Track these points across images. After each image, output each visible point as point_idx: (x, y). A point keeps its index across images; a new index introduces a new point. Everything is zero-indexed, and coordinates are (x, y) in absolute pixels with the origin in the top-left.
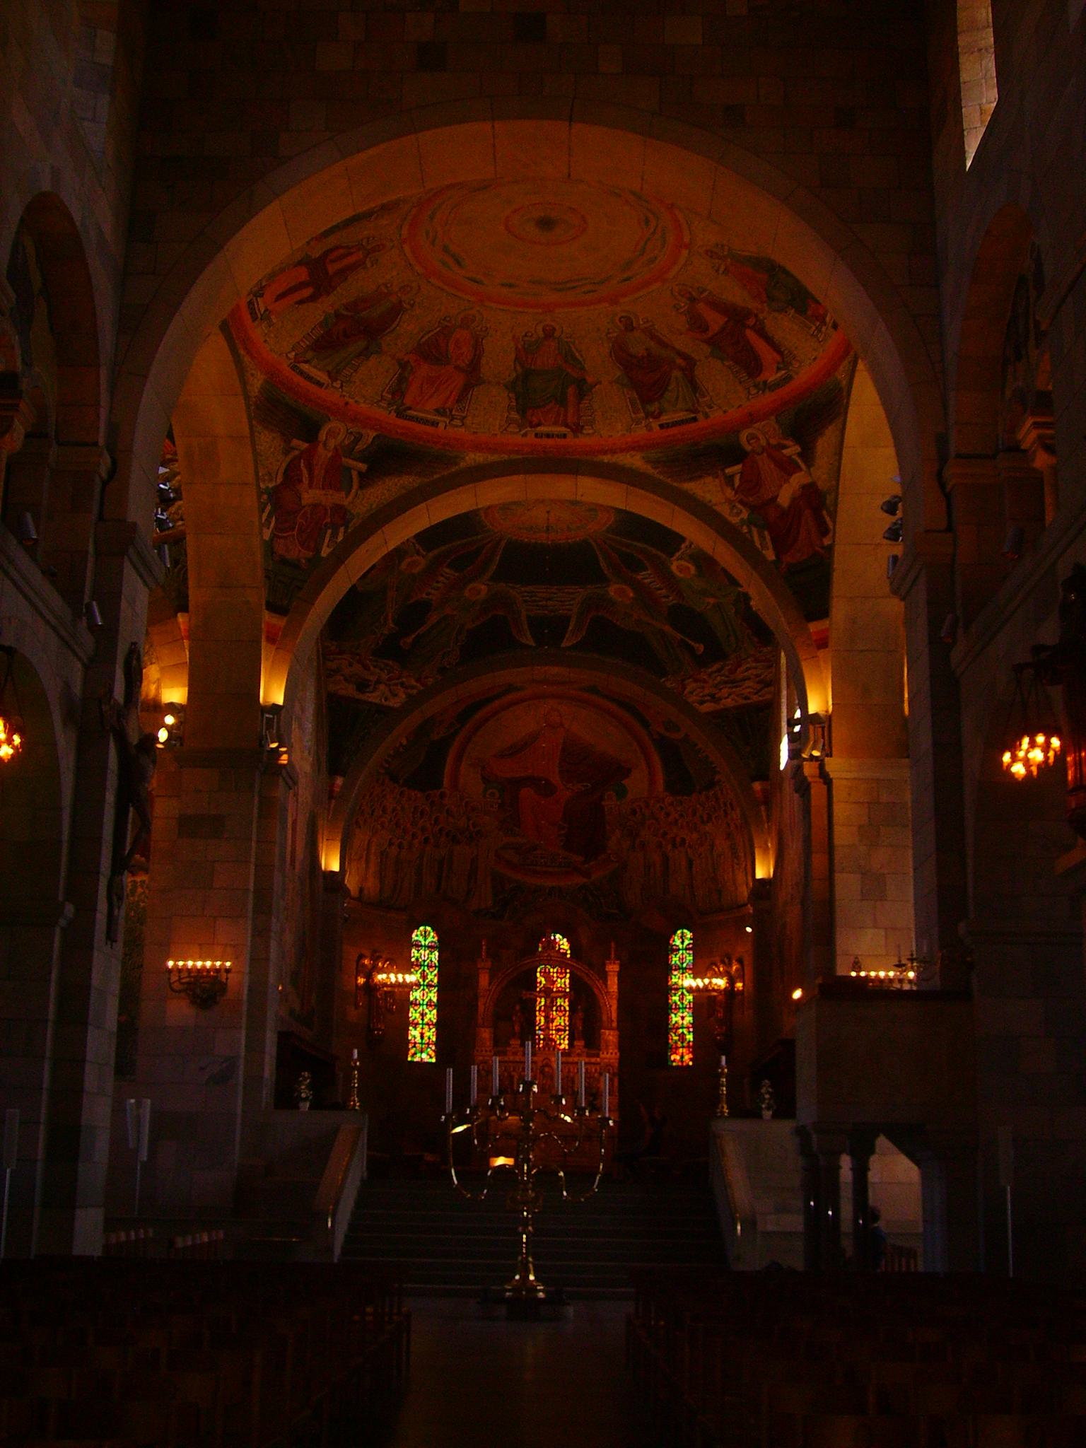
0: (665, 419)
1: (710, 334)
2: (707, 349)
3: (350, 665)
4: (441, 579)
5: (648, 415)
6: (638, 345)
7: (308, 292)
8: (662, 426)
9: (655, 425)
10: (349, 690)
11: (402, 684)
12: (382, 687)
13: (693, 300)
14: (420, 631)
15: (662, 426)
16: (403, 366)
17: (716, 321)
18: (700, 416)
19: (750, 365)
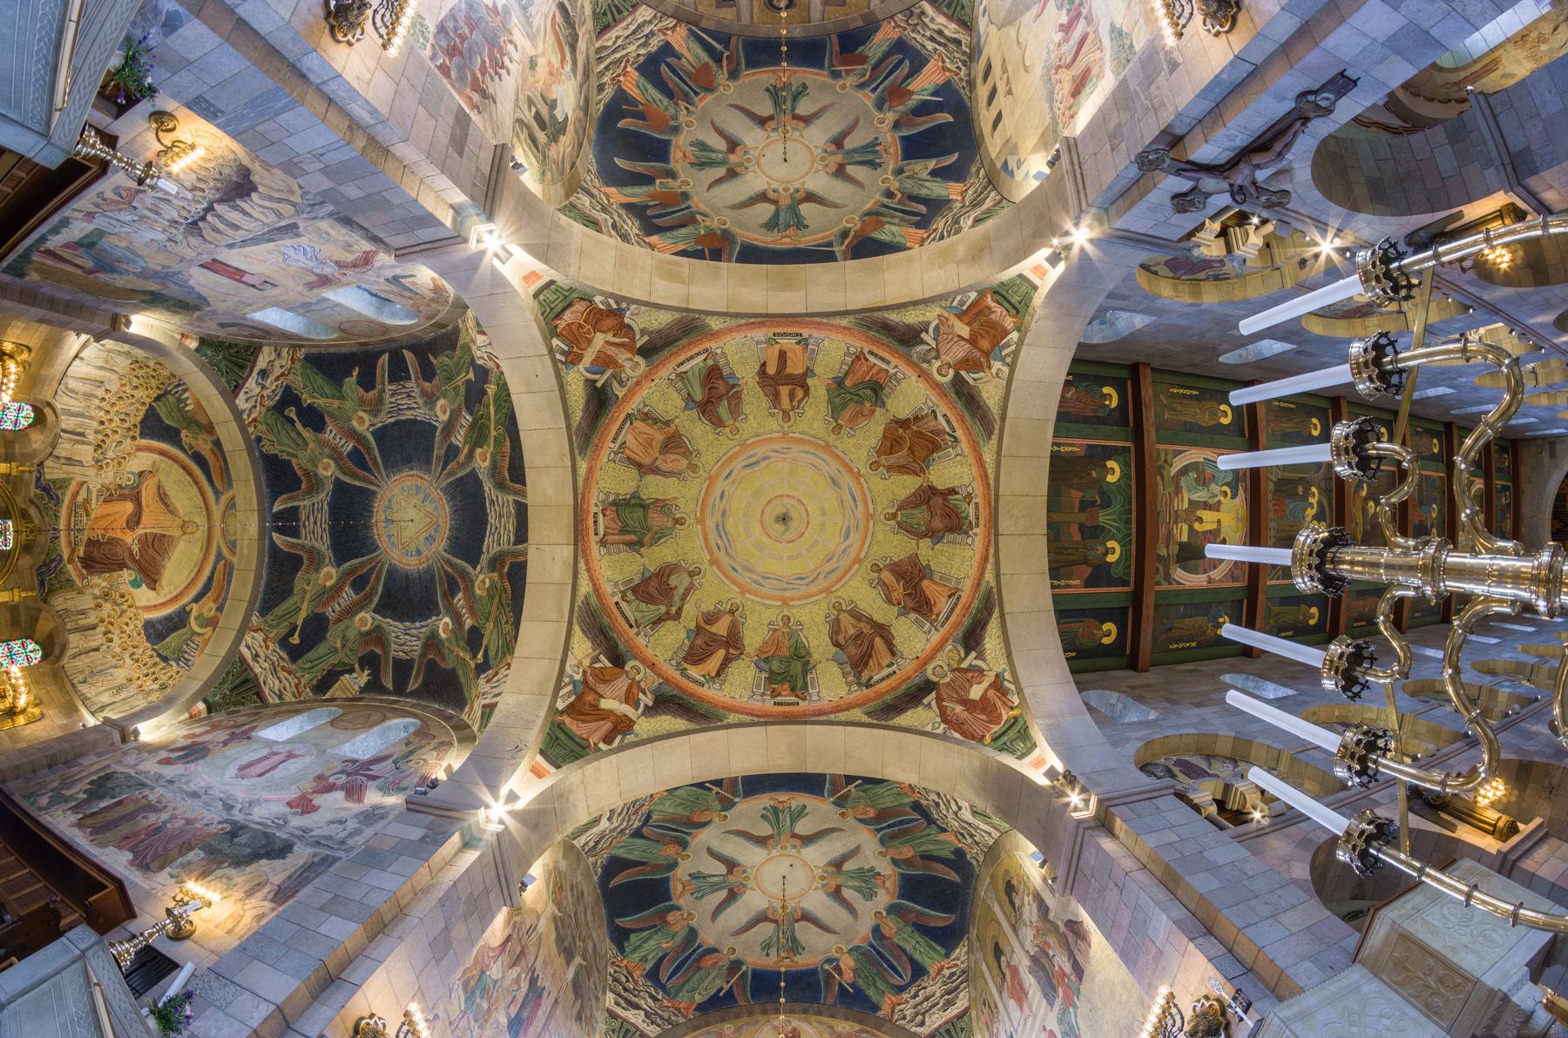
0: (623, 605)
1: (708, 627)
2: (692, 626)
3: (281, 367)
4: (343, 442)
5: (624, 595)
6: (679, 581)
7: (771, 370)
8: (617, 603)
9: (617, 598)
10: (262, 363)
11: (255, 407)
12: (258, 390)
13: (732, 612)
14: (298, 425)
15: (617, 603)
16: (667, 423)
17: (721, 628)
18: (635, 630)
19: (695, 656)
